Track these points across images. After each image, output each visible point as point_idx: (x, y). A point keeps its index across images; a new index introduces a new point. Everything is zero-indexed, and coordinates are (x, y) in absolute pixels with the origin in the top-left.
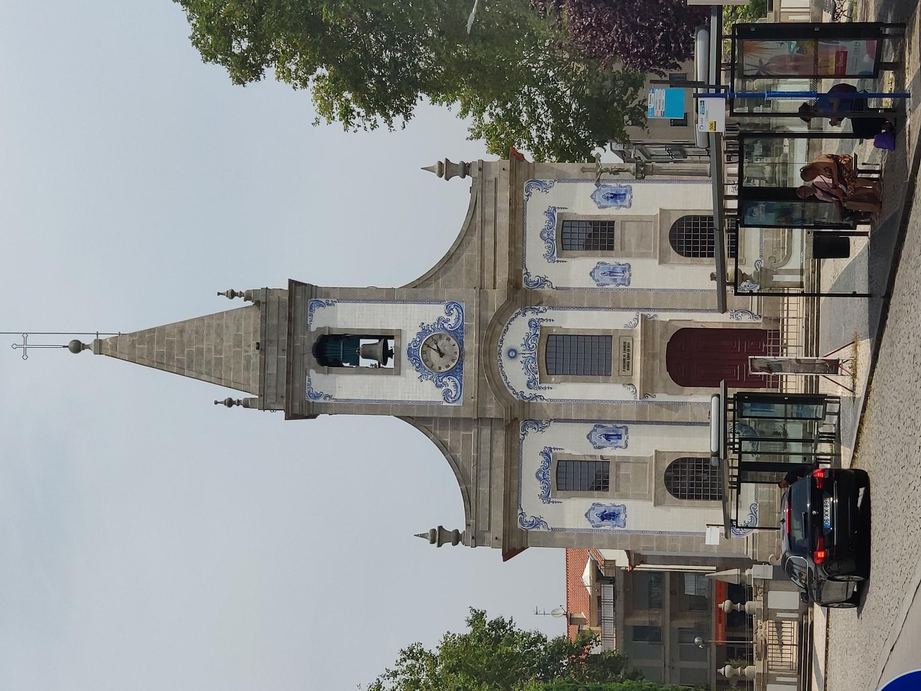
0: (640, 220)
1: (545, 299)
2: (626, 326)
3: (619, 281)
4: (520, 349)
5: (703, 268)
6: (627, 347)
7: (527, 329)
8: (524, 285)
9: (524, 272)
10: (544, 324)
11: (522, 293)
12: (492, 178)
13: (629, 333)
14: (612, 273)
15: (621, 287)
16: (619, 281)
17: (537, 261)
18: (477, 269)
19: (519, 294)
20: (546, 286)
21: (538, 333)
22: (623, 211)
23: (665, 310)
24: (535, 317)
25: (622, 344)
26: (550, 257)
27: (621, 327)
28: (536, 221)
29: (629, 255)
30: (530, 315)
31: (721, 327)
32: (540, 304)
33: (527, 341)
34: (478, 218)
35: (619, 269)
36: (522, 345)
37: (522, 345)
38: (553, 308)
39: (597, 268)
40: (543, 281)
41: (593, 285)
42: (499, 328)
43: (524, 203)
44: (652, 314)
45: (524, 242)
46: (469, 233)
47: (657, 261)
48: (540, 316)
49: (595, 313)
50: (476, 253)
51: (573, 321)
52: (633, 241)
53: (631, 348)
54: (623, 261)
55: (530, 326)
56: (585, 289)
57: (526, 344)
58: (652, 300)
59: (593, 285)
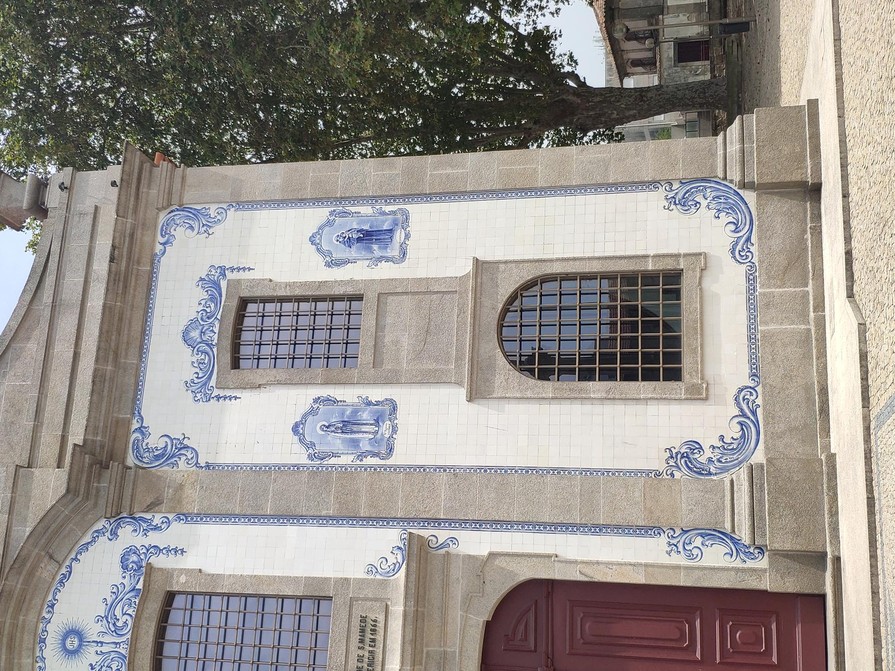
0: (423, 291)
1: (169, 493)
2: (372, 569)
3: (365, 446)
4: (93, 630)
5: (587, 408)
6: (368, 632)
7: (115, 575)
8: (131, 460)
9: (135, 425)
10: (160, 561)
11: (111, 474)
12: (87, 206)
13: (373, 589)
14: (347, 425)
15: (370, 461)
16: (365, 446)
17: (169, 401)
18: (28, 423)
19: (106, 484)
20: (182, 463)
21: (140, 586)
22: (385, 271)
23: (479, 524)
24: (139, 541)
25: (356, 623)
26: (200, 389)
27: (357, 572)
28: (177, 301)
29: (392, 379)
30: (128, 536)
31: (639, 578)
32: (150, 508)
33: (111, 607)
34: (47, 296)
35: (365, 416)
36: (99, 619)
37: (99, 619)
38: (186, 517)
39: (312, 412)
40: (179, 448)
41: (300, 456)
42: (46, 570)
43: (154, 261)
44: (443, 535)
45: (142, 352)
46: (21, 335)
47: (462, 393)
48: (154, 538)
49: (291, 531)
50: (32, 383)
51: (219, 553)
52: (406, 342)
53: (380, 637)
54: (377, 394)
55: (125, 567)
56: (279, 467)
57: (109, 617)
58: (443, 493)
59: (300, 456)
